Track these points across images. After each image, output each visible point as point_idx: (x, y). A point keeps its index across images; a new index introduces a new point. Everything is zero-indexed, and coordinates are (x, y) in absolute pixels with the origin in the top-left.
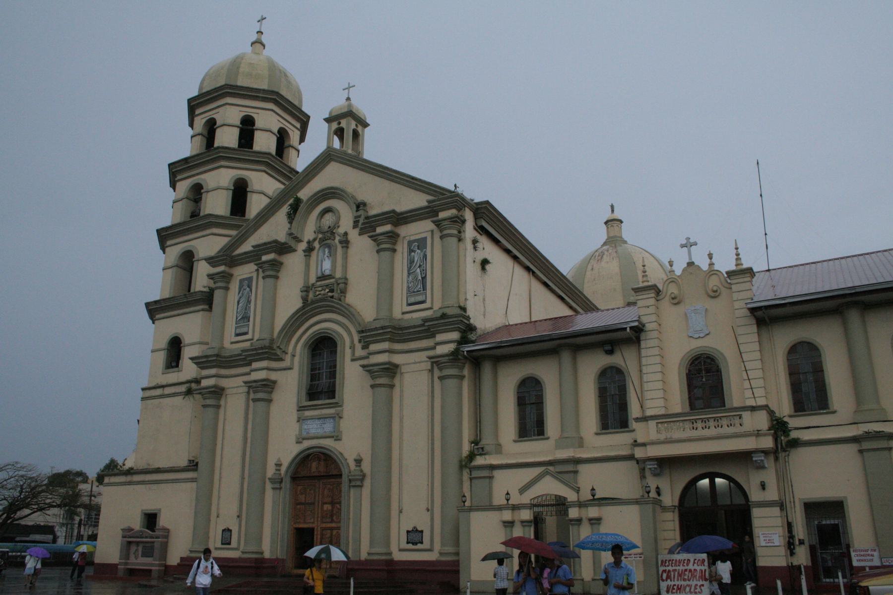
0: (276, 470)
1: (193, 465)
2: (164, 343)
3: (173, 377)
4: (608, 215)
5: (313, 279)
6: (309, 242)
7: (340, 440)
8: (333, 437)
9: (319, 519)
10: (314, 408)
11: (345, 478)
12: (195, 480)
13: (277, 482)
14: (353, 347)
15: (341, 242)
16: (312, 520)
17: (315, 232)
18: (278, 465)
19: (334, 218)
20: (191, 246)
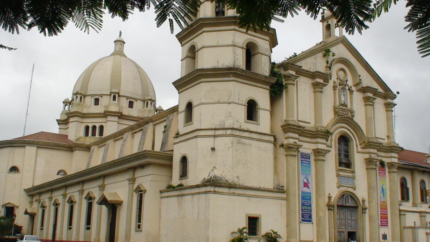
0: (329, 200)
1: (280, 189)
2: (245, 101)
3: (251, 126)
4: (117, 37)
5: (338, 104)
6: (334, 82)
7: (355, 190)
8: (352, 188)
9: (347, 227)
10: (342, 170)
11: (360, 209)
12: (286, 199)
13: (330, 207)
14: (357, 146)
15: (349, 89)
16: (343, 227)
17: (337, 79)
18: (330, 198)
19: (344, 75)
20: (255, 41)
